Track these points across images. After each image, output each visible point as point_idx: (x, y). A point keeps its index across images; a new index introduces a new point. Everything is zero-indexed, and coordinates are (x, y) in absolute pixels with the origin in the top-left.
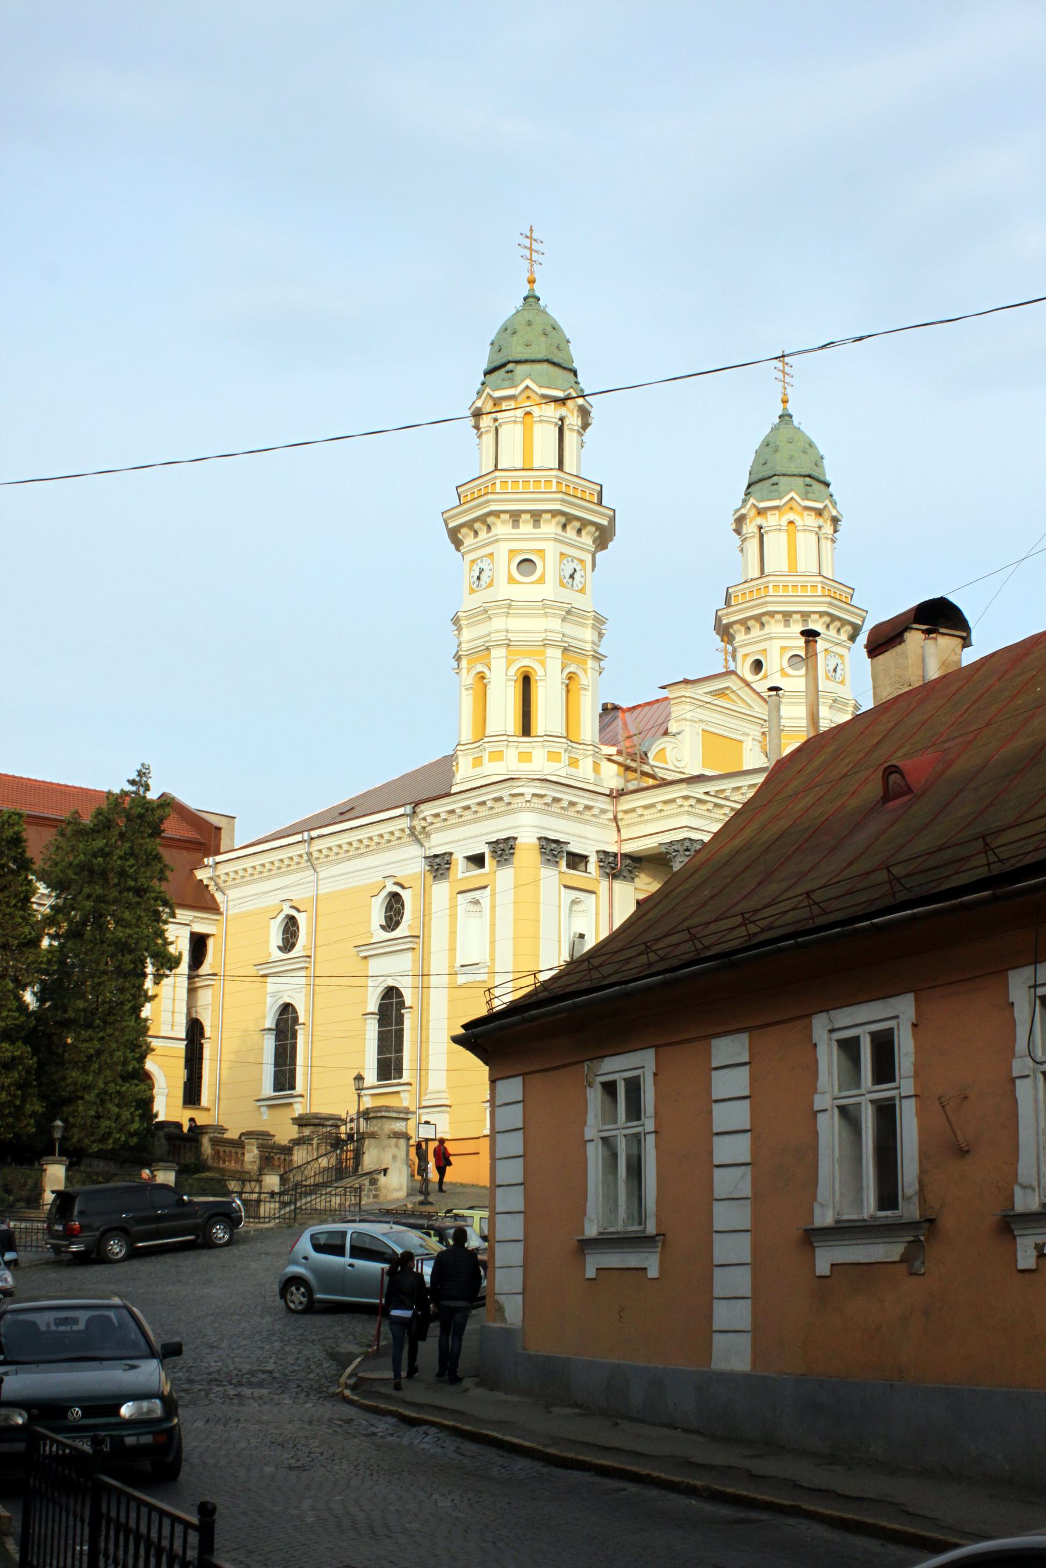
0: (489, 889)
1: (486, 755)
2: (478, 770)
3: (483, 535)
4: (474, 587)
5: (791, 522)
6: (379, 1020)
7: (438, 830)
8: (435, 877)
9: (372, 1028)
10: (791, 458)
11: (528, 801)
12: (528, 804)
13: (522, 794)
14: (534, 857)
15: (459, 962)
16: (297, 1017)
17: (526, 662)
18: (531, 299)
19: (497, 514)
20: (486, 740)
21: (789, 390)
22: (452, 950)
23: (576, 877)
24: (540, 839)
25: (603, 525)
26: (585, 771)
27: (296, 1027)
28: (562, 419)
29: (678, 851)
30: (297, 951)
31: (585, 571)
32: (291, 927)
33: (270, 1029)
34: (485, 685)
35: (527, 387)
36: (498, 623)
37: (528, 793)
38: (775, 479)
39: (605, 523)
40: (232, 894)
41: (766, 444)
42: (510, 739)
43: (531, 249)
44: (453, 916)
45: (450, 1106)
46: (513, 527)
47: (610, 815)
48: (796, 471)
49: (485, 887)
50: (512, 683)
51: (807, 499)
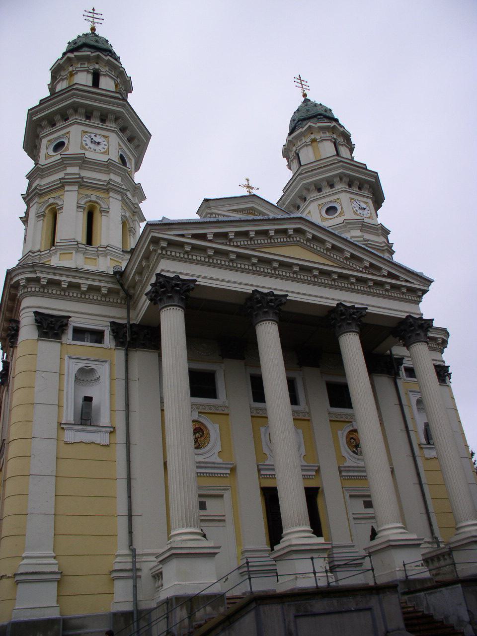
5: (314, 141)
11: (24, 287)
12: (26, 290)
13: (18, 282)
17: (51, 201)
23: (86, 347)
31: (108, 142)
38: (299, 123)
47: (122, 294)
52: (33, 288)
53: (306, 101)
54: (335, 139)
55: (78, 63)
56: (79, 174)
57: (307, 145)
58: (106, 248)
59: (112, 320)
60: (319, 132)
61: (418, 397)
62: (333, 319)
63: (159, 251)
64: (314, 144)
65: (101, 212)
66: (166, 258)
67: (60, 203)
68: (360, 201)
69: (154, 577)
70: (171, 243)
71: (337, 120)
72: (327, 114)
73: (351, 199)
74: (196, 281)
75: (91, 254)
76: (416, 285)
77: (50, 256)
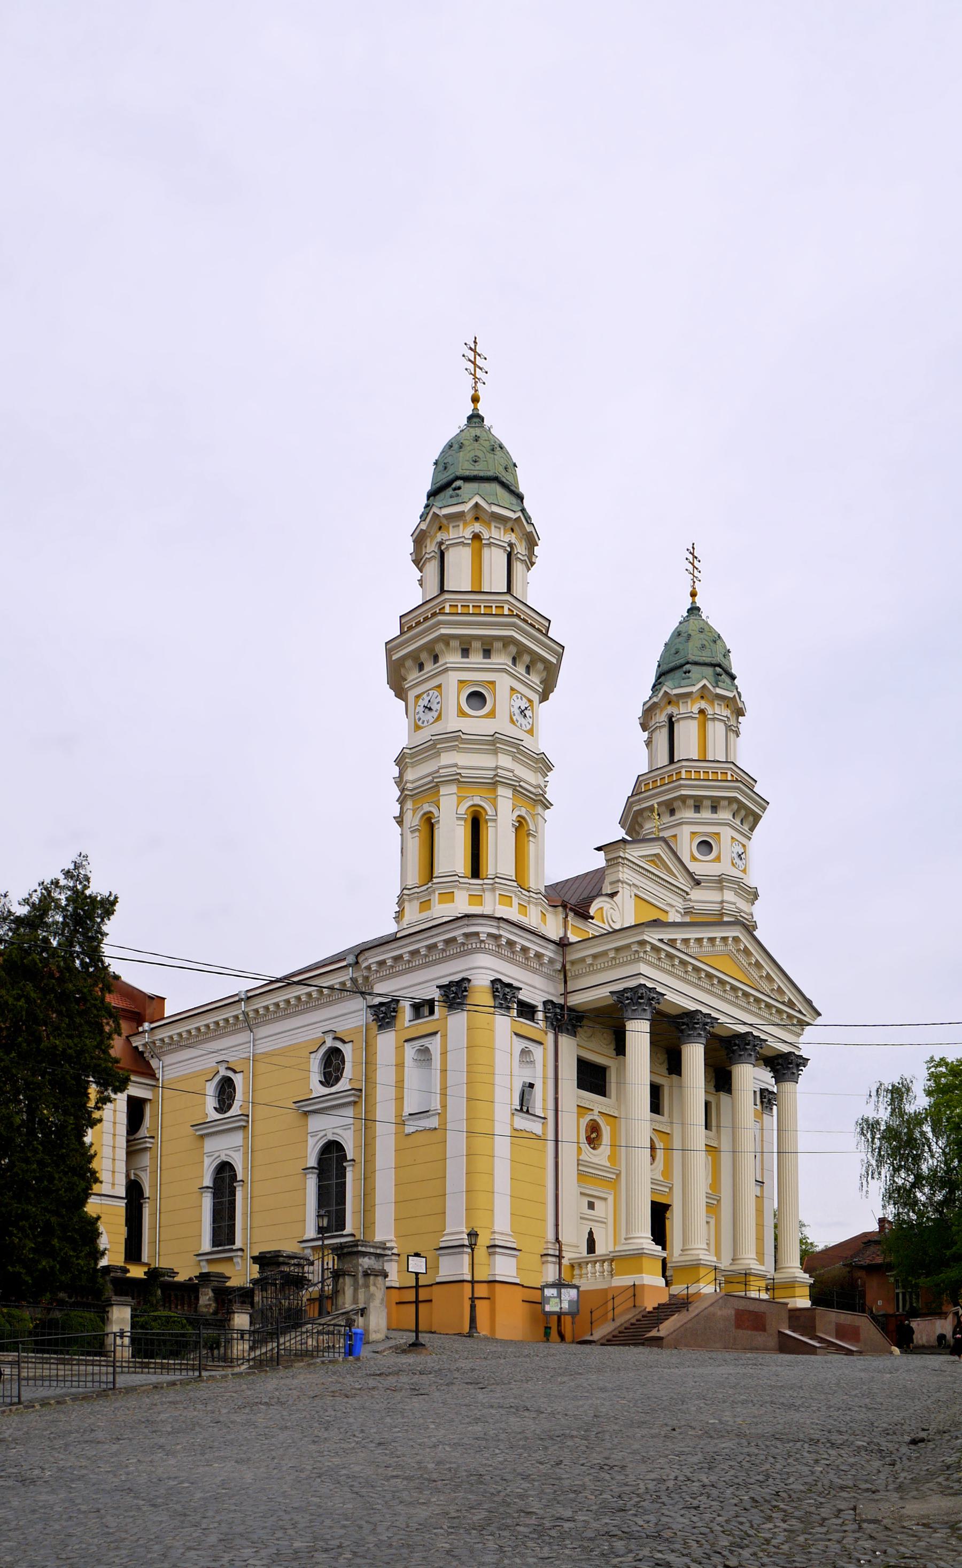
1: (435, 897)
2: (425, 915)
5: (702, 712)
10: (703, 646)
11: (483, 941)
13: (477, 934)
14: (487, 999)
20: (435, 880)
24: (493, 982)
26: (532, 919)
34: (432, 827)
37: (483, 933)
38: (688, 667)
41: (677, 634)
42: (462, 880)
47: (558, 966)
48: (708, 660)
52: (491, 945)
53: (694, 610)
58: (536, 893)
59: (551, 998)
64: (702, 717)
66: (645, 963)
70: (655, 949)
71: (733, 678)
72: (724, 663)
75: (524, 900)
77: (483, 890)
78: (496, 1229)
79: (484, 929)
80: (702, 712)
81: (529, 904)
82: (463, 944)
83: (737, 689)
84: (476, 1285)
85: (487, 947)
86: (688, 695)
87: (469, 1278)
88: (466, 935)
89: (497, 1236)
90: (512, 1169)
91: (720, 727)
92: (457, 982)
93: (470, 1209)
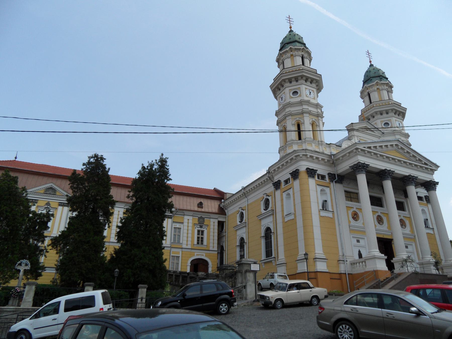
0: (292, 189)
1: (287, 148)
3: (282, 89)
4: (281, 104)
5: (378, 89)
6: (265, 239)
7: (276, 175)
8: (276, 189)
9: (263, 242)
10: (375, 73)
11: (301, 157)
12: (302, 159)
13: (299, 155)
15: (285, 214)
16: (244, 241)
17: (298, 119)
18: (291, 31)
19: (284, 80)
20: (287, 143)
21: (371, 60)
22: (283, 211)
25: (318, 80)
27: (244, 244)
28: (302, 55)
29: (357, 167)
30: (244, 221)
32: (242, 215)
33: (238, 246)
35: (291, 48)
36: (287, 110)
37: (301, 154)
38: (372, 78)
39: (319, 79)
40: (229, 209)
41: (367, 72)
42: (295, 142)
43: (289, 20)
44: (282, 200)
45: (286, 264)
46: (290, 83)
47: (331, 162)
49: (291, 188)
50: (294, 126)
51: (381, 81)
52: (304, 158)
53: (371, 65)
54: (387, 89)
55: (295, 51)
56: (308, 109)
57: (375, 91)
59: (329, 172)
60: (381, 85)
61: (422, 208)
62: (405, 180)
63: (358, 153)
64: (378, 90)
65: (317, 126)
67: (302, 121)
68: (398, 121)
69: (351, 264)
70: (362, 150)
71: (387, 79)
72: (383, 75)
73: (396, 120)
74: (369, 165)
76: (434, 168)
77: (302, 143)
78: (316, 252)
79: (301, 154)
80: (378, 89)
81: (319, 145)
82: (295, 159)
83: (389, 81)
84: (309, 273)
85: (303, 158)
86: (373, 85)
87: (306, 271)
88: (296, 156)
89: (316, 255)
90: (321, 230)
91: (385, 93)
92: (295, 171)
93: (306, 246)
